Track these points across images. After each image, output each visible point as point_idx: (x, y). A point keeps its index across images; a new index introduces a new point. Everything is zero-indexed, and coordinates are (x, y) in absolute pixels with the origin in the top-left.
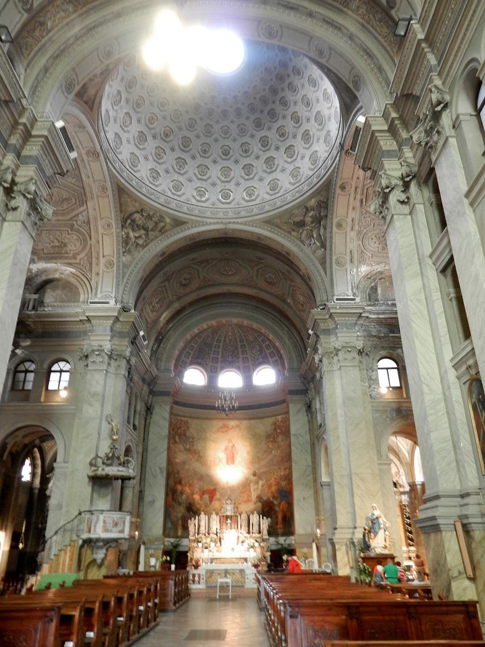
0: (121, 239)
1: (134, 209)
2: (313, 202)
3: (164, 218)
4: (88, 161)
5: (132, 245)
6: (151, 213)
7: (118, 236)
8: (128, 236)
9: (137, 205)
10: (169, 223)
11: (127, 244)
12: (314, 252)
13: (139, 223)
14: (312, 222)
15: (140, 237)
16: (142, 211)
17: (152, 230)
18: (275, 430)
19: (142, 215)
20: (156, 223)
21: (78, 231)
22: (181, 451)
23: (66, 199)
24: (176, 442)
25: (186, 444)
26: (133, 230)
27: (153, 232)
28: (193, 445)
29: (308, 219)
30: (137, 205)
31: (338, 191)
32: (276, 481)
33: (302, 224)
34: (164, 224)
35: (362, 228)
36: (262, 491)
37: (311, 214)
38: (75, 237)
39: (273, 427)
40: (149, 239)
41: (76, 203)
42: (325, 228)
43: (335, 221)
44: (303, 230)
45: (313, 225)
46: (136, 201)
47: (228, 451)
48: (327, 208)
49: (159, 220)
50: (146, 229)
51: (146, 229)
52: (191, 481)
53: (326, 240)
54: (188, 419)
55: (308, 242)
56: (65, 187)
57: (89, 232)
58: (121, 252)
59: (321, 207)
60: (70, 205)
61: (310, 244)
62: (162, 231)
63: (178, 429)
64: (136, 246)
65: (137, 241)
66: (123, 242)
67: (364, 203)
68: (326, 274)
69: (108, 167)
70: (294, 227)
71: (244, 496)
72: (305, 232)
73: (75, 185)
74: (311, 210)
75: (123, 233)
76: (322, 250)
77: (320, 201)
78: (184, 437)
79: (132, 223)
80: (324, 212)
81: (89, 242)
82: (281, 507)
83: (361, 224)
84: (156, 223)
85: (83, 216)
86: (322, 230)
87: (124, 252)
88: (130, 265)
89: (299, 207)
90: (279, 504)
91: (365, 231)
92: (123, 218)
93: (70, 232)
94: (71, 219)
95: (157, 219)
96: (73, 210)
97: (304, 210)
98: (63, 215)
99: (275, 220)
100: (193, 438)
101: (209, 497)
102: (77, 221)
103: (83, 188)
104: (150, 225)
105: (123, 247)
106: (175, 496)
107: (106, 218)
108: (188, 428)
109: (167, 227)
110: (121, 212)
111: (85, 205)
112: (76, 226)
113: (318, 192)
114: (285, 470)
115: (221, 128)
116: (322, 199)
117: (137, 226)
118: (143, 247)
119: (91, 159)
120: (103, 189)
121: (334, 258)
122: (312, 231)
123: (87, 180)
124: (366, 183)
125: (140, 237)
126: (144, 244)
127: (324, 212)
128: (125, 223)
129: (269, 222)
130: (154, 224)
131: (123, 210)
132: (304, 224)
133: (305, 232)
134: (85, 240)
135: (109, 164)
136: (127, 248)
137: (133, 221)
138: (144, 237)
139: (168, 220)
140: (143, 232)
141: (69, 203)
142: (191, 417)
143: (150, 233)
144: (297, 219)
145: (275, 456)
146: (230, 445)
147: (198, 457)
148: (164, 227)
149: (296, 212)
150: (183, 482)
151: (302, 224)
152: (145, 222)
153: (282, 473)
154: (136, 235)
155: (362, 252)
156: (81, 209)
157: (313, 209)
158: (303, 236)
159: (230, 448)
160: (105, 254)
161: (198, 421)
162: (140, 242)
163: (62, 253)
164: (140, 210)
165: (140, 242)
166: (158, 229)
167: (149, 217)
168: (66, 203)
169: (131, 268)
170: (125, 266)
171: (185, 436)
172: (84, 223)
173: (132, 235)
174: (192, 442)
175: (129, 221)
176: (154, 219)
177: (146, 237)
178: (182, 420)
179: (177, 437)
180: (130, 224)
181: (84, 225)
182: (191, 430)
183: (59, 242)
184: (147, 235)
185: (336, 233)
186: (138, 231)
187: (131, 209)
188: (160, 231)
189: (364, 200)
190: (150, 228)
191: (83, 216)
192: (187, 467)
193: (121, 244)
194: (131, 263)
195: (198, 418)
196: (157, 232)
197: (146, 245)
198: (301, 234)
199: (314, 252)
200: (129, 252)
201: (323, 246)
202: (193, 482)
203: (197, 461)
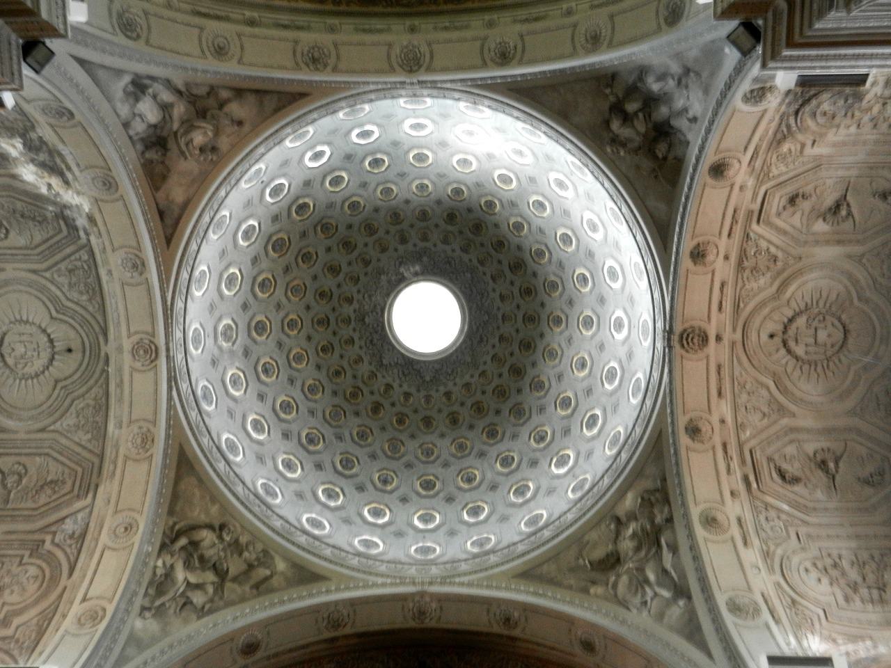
0: (147, 576)
1: (203, 518)
2: (630, 501)
3: (272, 558)
4: (133, 369)
5: (174, 599)
6: (243, 540)
7: (143, 560)
8: (169, 574)
9: (214, 509)
10: (282, 573)
12: (660, 617)
13: (209, 553)
14: (638, 549)
15: (199, 587)
17: (234, 580)
19: (220, 538)
20: (251, 567)
21: (50, 558)
23: (51, 482)
26: (188, 565)
27: (235, 586)
29: (626, 545)
30: (214, 509)
31: (684, 440)
33: (612, 562)
34: (268, 572)
35: (772, 548)
37: (630, 531)
38: (33, 571)
40: (221, 598)
41: (72, 491)
42: (674, 549)
43: (695, 512)
44: (618, 576)
45: (643, 553)
48: (667, 501)
49: (258, 559)
50: (222, 574)
51: (222, 574)
53: (683, 576)
55: (637, 600)
56: (61, 454)
57: (72, 559)
58: (139, 601)
59: (652, 505)
60: (54, 497)
61: (646, 603)
62: (261, 587)
64: (185, 604)
65: (189, 594)
66: (150, 584)
67: (754, 485)
69: (170, 398)
70: (596, 575)
72: (624, 579)
73: (84, 448)
75: (160, 563)
77: (647, 491)
79: (190, 548)
80: (662, 512)
81: (63, 582)
83: (763, 534)
84: (251, 567)
86: (667, 558)
87: (143, 609)
88: (148, 646)
89: (598, 523)
91: (779, 552)
92: (172, 528)
93: (26, 560)
94: (42, 530)
95: (254, 556)
96: (58, 508)
97: (613, 526)
98: (28, 519)
99: (545, 567)
102: (54, 533)
103: (102, 457)
104: (235, 566)
105: (146, 594)
107: (130, 509)
109: (275, 582)
110: (171, 512)
112: (48, 546)
113: (638, 473)
115: (420, 446)
117: (202, 559)
118: (202, 612)
119: (138, 365)
120: (145, 441)
121: (721, 600)
122: (641, 570)
123: (117, 432)
124: (743, 437)
125: (199, 587)
126: (207, 607)
127: (662, 512)
128: (173, 541)
129: (529, 574)
130: (244, 567)
131: (178, 508)
132: (618, 560)
133: (624, 579)
134: (55, 579)
135: (174, 393)
136: (158, 603)
137: (195, 544)
138: (210, 590)
139: (281, 565)
140: (210, 577)
141: (55, 492)
143: (228, 585)
144: (599, 553)
148: (267, 579)
149: (593, 536)
151: (612, 562)
152: (222, 554)
154: (193, 580)
155: (794, 601)
156: (79, 505)
157: (632, 516)
158: (621, 589)
160: (91, 594)
162: (198, 598)
164: (217, 524)
165: (198, 598)
166: (252, 582)
168: (49, 492)
169: (148, 654)
170: (135, 641)
173: (180, 574)
175: (183, 541)
176: (246, 554)
180: (183, 548)
181: (69, 542)
184: (219, 587)
185: (706, 540)
186: (198, 572)
187: (197, 514)
188: (257, 586)
189: (752, 478)
190: (233, 571)
191: (75, 522)
193: (145, 585)
194: (154, 640)
196: (247, 588)
197: (211, 612)
198: (615, 586)
199: (660, 617)
200: (160, 612)
201: (681, 591)
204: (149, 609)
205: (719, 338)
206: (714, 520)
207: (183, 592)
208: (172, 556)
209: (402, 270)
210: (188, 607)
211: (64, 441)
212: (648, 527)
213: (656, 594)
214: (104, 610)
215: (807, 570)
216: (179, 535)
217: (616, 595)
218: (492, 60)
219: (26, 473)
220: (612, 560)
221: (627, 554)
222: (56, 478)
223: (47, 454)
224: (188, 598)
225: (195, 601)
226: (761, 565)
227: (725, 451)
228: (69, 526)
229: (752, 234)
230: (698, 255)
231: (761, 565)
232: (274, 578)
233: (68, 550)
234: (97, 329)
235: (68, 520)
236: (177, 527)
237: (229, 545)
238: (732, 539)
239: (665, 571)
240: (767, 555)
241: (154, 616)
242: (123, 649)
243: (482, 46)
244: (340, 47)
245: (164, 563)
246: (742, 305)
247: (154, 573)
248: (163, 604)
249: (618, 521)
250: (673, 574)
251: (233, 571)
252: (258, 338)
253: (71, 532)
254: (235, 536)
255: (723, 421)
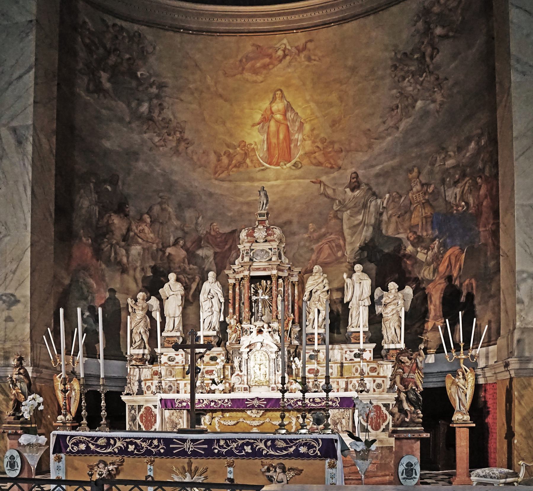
18: (428, 31)
22: (121, 120)
24: (99, 89)
25: (140, 102)
28: (161, 107)
32: (425, 193)
36: (377, 227)
39: (420, 25)
47: (272, 123)
52: (156, 209)
54: (143, 28)
63: (109, 52)
71: (320, 251)
78: (134, 84)
82: (442, 268)
90: (437, 259)
100: (161, 86)
101: (215, 253)
106: (106, 247)
108: (143, 55)
114: (460, 149)
142: (149, 24)
145: (425, 114)
146: (278, 106)
147: (179, 141)
150: (132, 210)
153: (450, 163)
159: (278, 116)
161: (178, 37)
171: (134, 75)
174: (158, 96)
178: (122, 28)
179: (104, 76)
182: (152, 60)
192: (141, 166)
195: (176, 29)
202: (163, 210)
203: (176, 152)
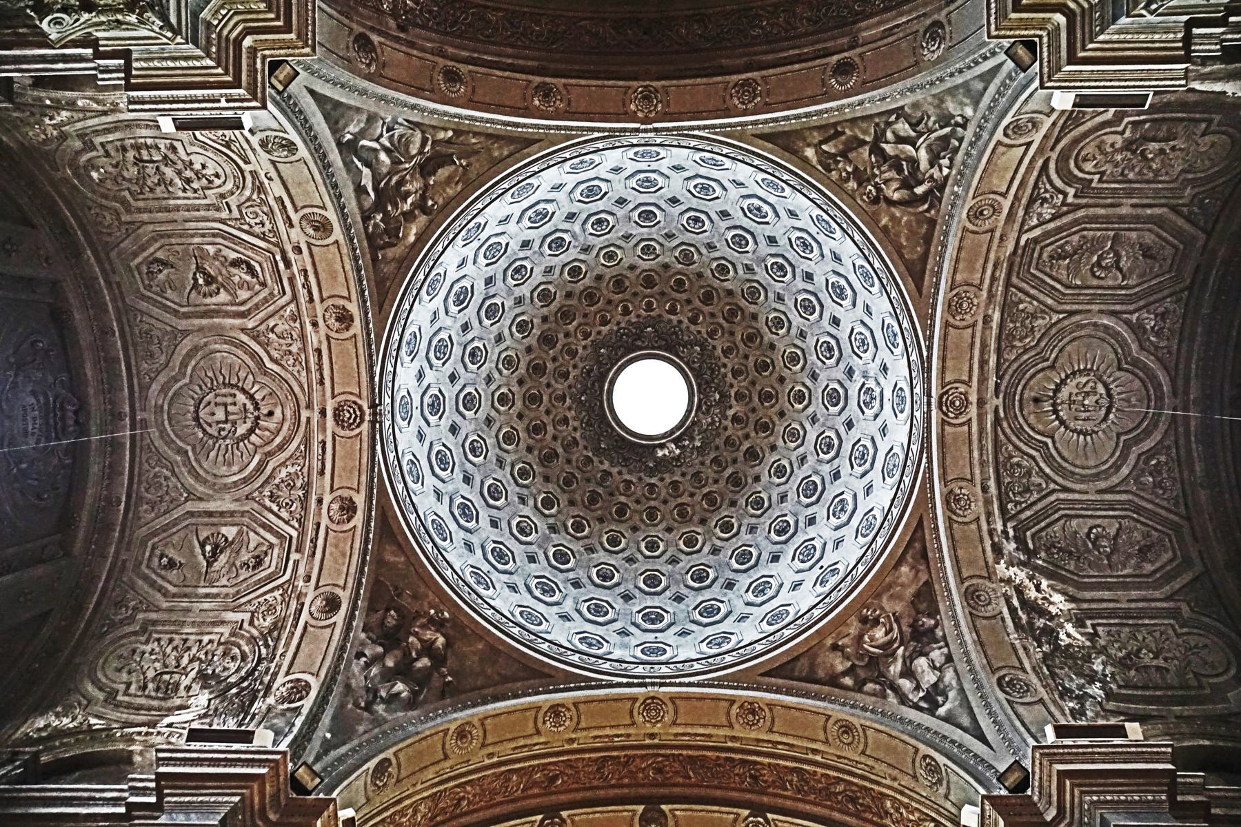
4: (968, 383)
5: (931, 131)
9: (884, 221)
10: (809, 145)
11: (945, 139)
13: (892, 174)
15: (900, 140)
16: (875, 201)
19: (879, 190)
26: (914, 162)
34: (824, 147)
35: (255, 197)
37: (410, 201)
40: (877, 125)
41: (1042, 248)
42: (360, 190)
44: (421, 152)
46: (885, 229)
48: (370, 238)
50: (876, 149)
51: (876, 149)
53: (348, 165)
56: (1053, 288)
62: (831, 131)
65: (913, 134)
66: (956, 150)
67: (278, 258)
68: (312, 92)
69: (930, 348)
72: (414, 151)
74: (411, 212)
75: (946, 171)
76: (348, 137)
79: (913, 183)
80: (376, 226)
84: (844, 153)
85: (1040, 215)
86: (367, 180)
87: (964, 126)
91: (247, 193)
93: (1097, 177)
94: (1079, 207)
97: (430, 203)
99: (506, 153)
102: (1064, 204)
105: (961, 140)
109: (817, 137)
110: (932, 223)
111: (1022, 243)
112: (1071, 191)
113: (404, 263)
116: (391, 253)
117: (900, 170)
118: (899, 112)
122: (396, 162)
124: (293, 306)
125: (900, 140)
126: (893, 118)
127: (376, 226)
128: (929, 192)
133: (414, 151)
135: (925, 354)
137: (906, 185)
138: (889, 135)
140: (888, 148)
154: (909, 147)
157: (409, 216)
162: (903, 128)
163: (1153, 121)
164: (883, 205)
165: (903, 128)
167: (861, 177)
169: (959, 80)
172: (1045, 200)
173: (923, 155)
175: (919, 190)
176: (850, 169)
177: (884, 132)
180: (920, 183)
181: (1048, 196)
183: (1143, 153)
184: (880, 137)
188: (838, 134)
190: (865, 152)
191: (1040, 215)
196: (848, 132)
197: (890, 112)
199: (372, 119)
200: (946, 119)
204: (957, 124)
205: (323, 413)
206: (316, 229)
207: (919, 137)
208: (932, 176)
209: (678, 452)
210: (914, 121)
211: (1050, 301)
212: (390, 208)
213: (377, 140)
214: (1006, 135)
215: (217, 176)
216: (923, 198)
217: (423, 132)
218: (569, 709)
219: (1093, 266)
220: (429, 168)
221: (412, 176)
222: (1061, 262)
223: (1067, 287)
224: (914, 131)
225: (907, 126)
226: (266, 182)
227: (310, 293)
228: (1047, 212)
229: (297, 525)
230: (349, 508)
231: (266, 182)
232: (816, 141)
233: (1048, 186)
234: (1005, 425)
235: (1048, 217)
236: (926, 206)
237: (868, 180)
238: (296, 211)
239: (368, 164)
240: (261, 189)
241: (953, 117)
242: (985, 89)
243: (578, 724)
244: (725, 723)
245: (941, 170)
246: (302, 447)
247: (951, 160)
248: (942, 127)
249: (425, 210)
250: (359, 164)
251: (865, 152)
252: (837, 386)
253: (1046, 205)
254: (862, 190)
255: (315, 324)
